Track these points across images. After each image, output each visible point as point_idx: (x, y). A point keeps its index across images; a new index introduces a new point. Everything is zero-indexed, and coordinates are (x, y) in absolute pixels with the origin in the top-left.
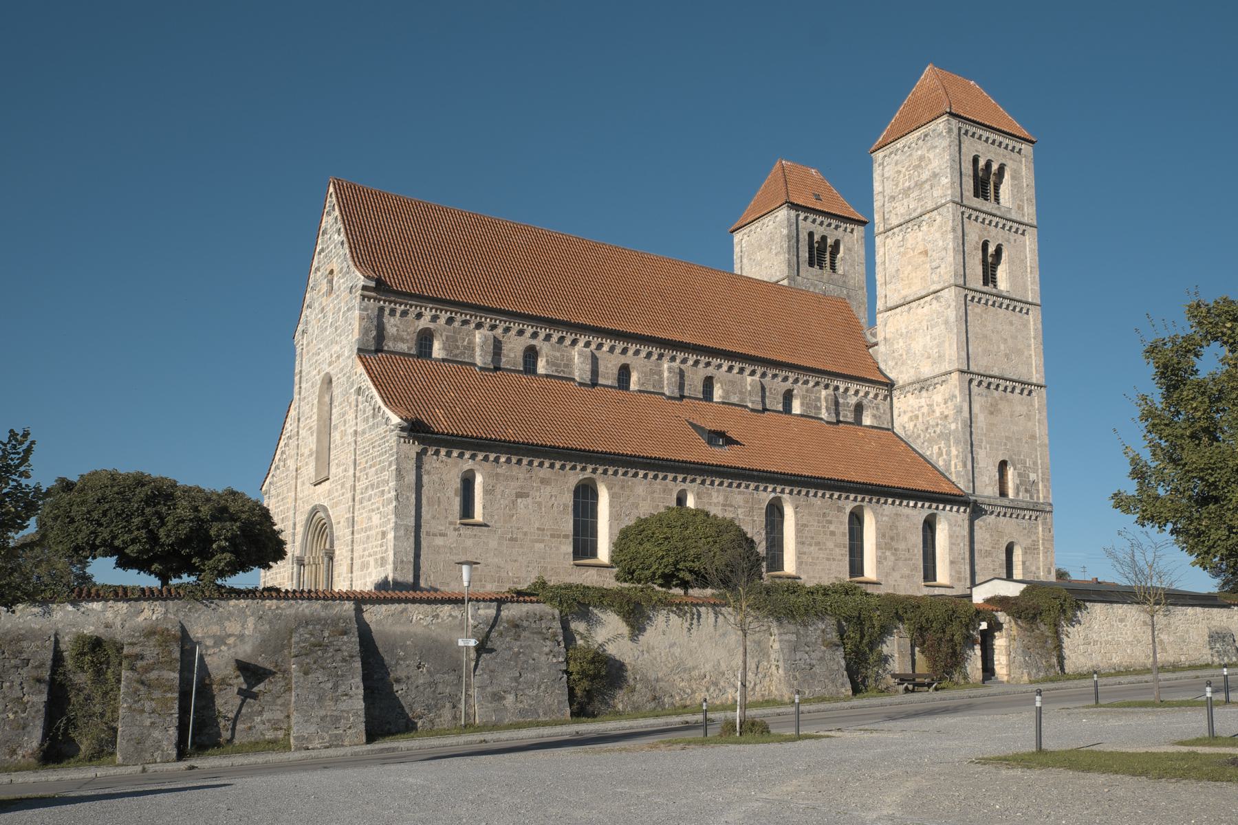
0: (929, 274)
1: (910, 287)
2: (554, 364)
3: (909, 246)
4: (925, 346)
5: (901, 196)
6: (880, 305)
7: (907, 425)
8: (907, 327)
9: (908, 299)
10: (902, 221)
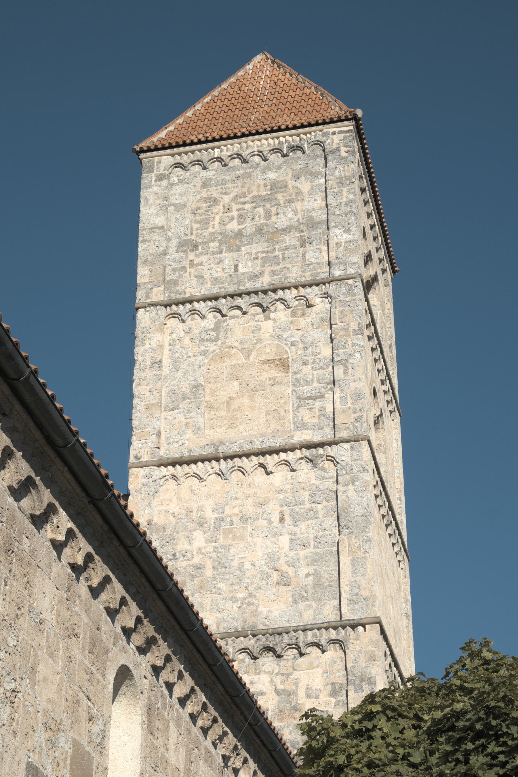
1: (232, 426)
3: (232, 341)
4: (272, 558)
5: (214, 245)
8: (219, 508)
9: (223, 450)
10: (215, 291)
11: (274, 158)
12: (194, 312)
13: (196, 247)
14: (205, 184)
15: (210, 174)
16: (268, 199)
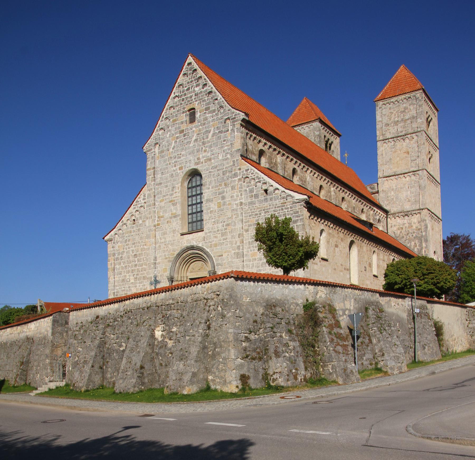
0: (410, 163)
1: (398, 168)
2: (302, 180)
4: (407, 196)
5: (392, 124)
6: (380, 174)
7: (396, 232)
9: (397, 173)
10: (393, 136)
11: (405, 100)
12: (389, 141)
13: (389, 125)
14: (390, 109)
15: (391, 106)
16: (404, 111)
